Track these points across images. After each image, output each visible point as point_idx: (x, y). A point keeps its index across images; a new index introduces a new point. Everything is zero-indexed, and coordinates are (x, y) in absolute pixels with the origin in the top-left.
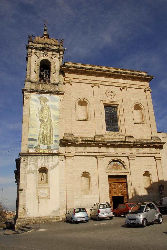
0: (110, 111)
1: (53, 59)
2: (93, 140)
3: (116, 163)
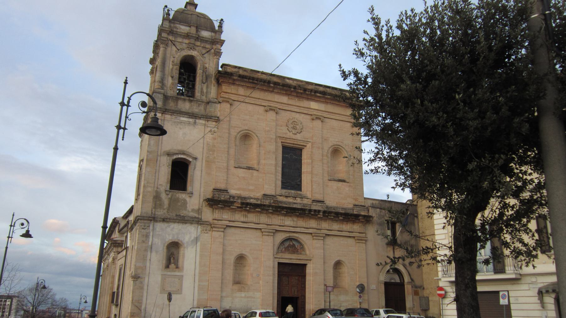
1: (203, 55)
2: (259, 202)
3: (291, 244)
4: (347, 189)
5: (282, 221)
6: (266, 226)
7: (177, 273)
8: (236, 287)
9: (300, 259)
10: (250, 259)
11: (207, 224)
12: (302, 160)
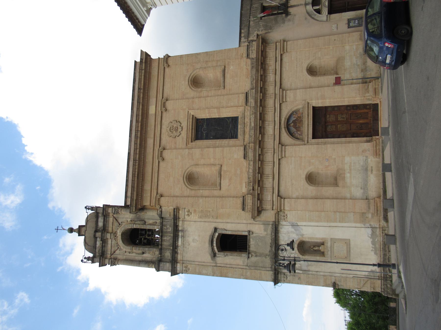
1: (120, 225)
2: (252, 163)
3: (292, 124)
4: (232, 67)
5: (270, 138)
7: (329, 244)
8: (340, 183)
9: (308, 115)
10: (310, 169)
11: (278, 216)
12: (207, 118)
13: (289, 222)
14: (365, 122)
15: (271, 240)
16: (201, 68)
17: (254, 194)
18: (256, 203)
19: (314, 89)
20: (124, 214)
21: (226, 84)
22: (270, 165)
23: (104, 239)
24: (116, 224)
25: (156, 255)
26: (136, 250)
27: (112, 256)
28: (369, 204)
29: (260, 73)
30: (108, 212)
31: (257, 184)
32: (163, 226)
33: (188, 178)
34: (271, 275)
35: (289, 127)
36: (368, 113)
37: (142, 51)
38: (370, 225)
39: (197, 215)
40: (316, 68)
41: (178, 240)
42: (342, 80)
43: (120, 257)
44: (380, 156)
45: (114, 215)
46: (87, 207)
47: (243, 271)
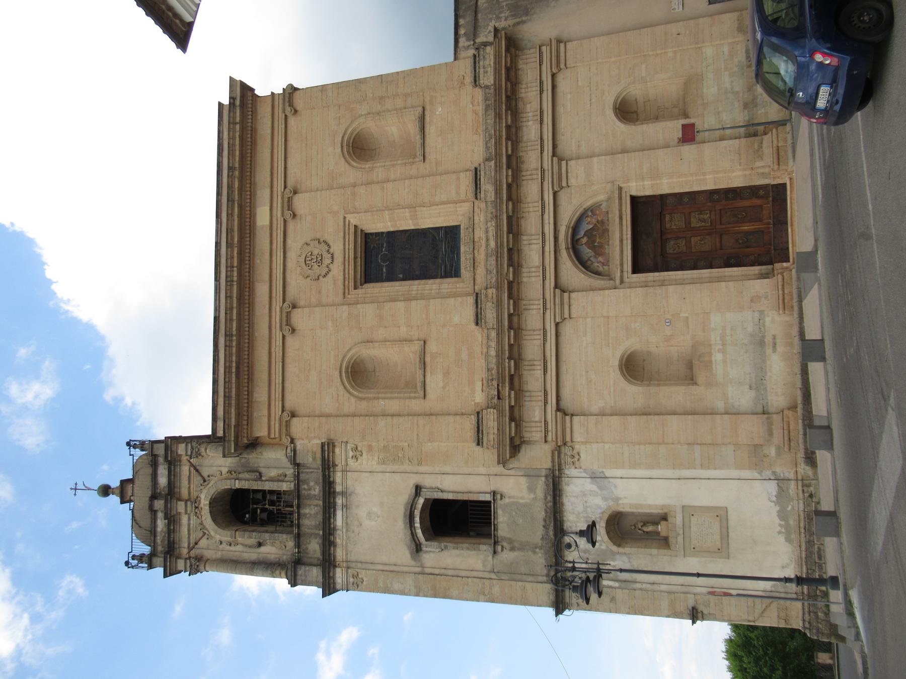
0: (385, 261)
2: (493, 334)
3: (585, 240)
4: (440, 109)
5: (534, 274)
6: (548, 311)
7: (679, 520)
8: (701, 377)
9: (621, 218)
11: (559, 456)
12: (389, 230)
13: (584, 470)
14: (755, 228)
15: (546, 510)
16: (369, 114)
17: (501, 409)
18: (508, 429)
19: (633, 154)
20: (212, 457)
21: (427, 149)
22: (535, 337)
23: (172, 514)
24: (197, 480)
25: (287, 548)
26: (243, 537)
27: (193, 553)
28: (770, 424)
29: (504, 121)
30: (177, 453)
31: (507, 385)
32: (301, 483)
33: (351, 372)
34: (549, 593)
35: (579, 247)
36: (761, 206)
37: (232, 80)
38: (774, 473)
39: (376, 458)
40: (637, 103)
41: (335, 515)
42: (698, 132)
43: (209, 554)
44: (793, 311)
45: (191, 461)
46: (132, 443)
47: (484, 584)
